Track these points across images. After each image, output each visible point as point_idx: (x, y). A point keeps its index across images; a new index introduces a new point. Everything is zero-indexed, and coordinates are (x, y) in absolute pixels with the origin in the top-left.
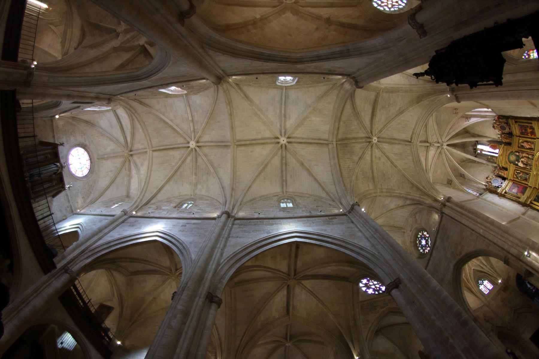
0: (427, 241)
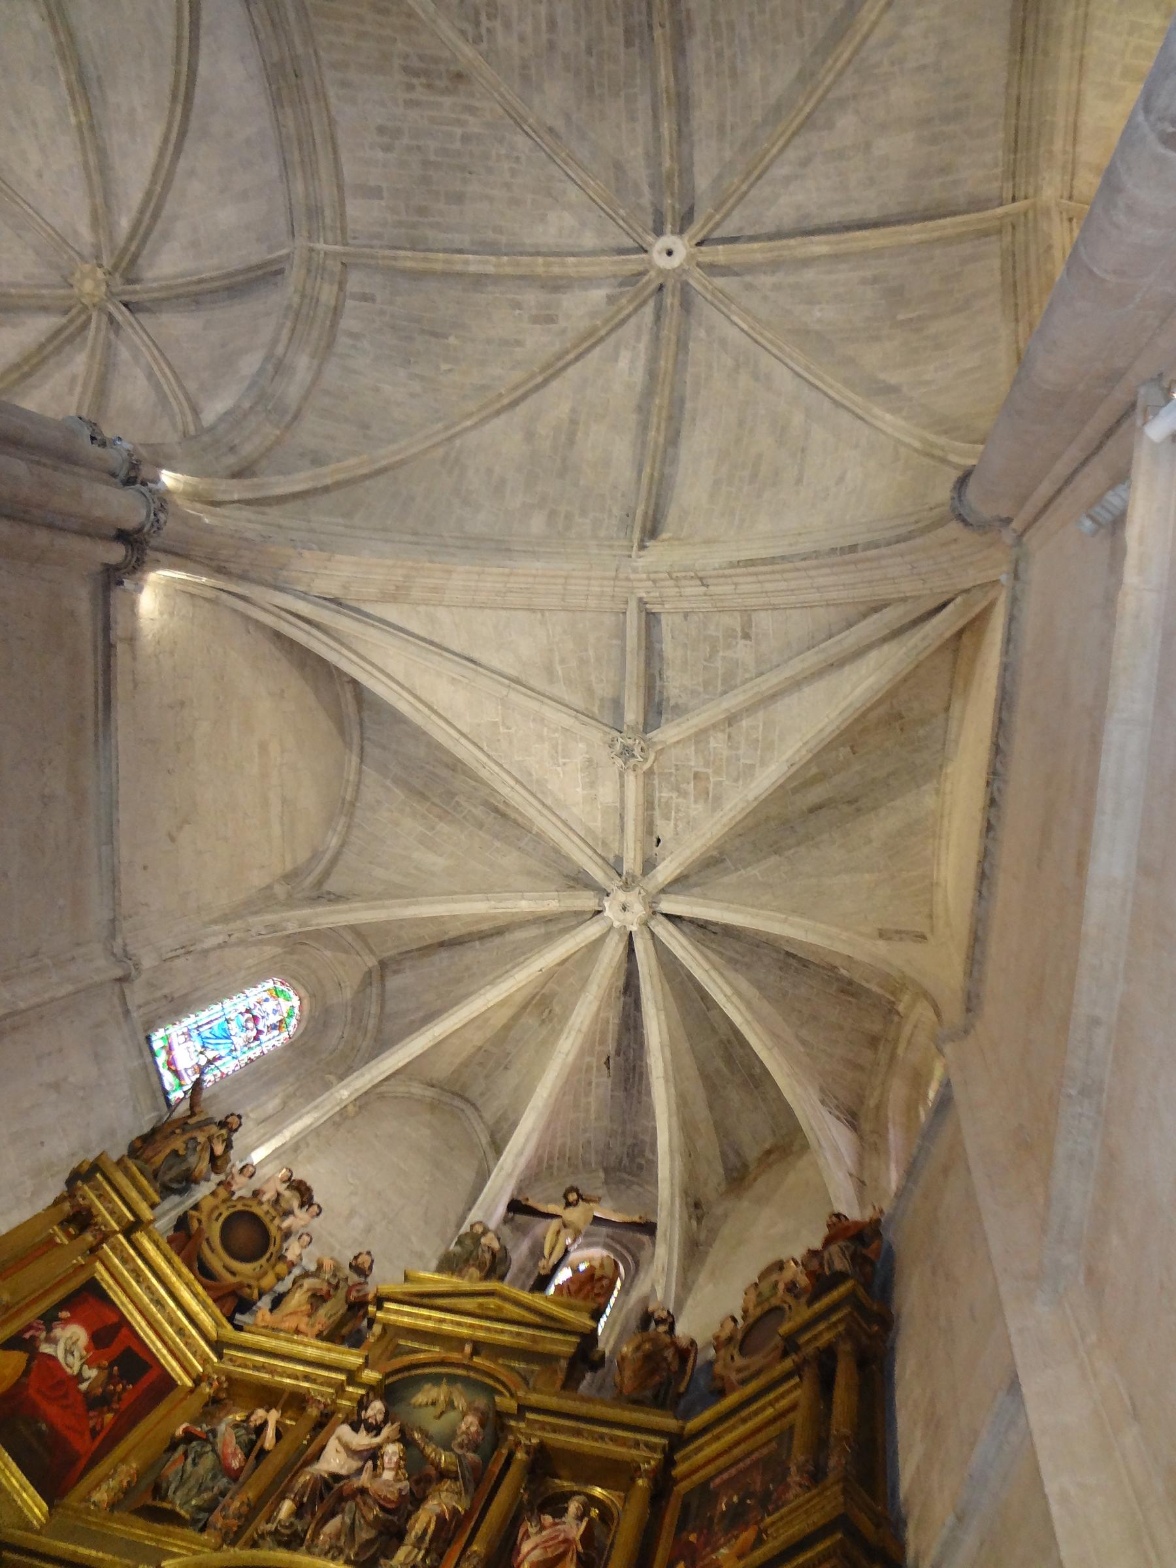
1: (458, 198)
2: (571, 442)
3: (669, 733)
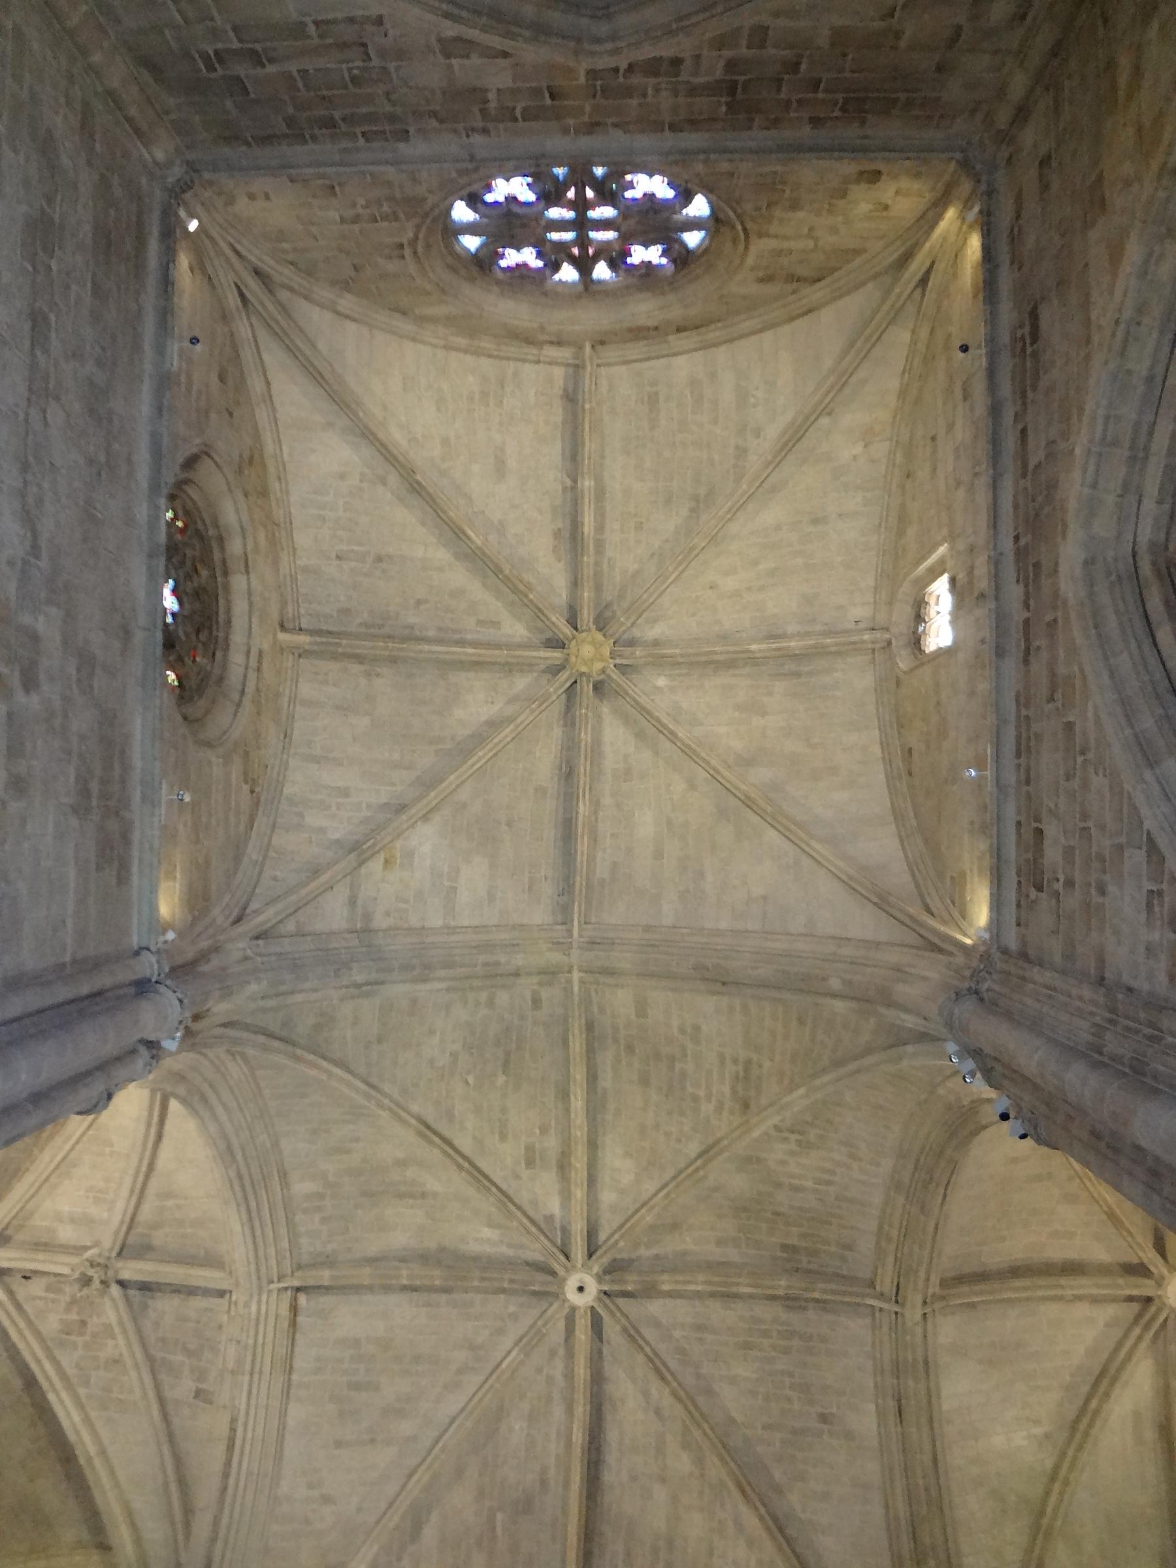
2: (401, 1196)
3: (111, 1310)
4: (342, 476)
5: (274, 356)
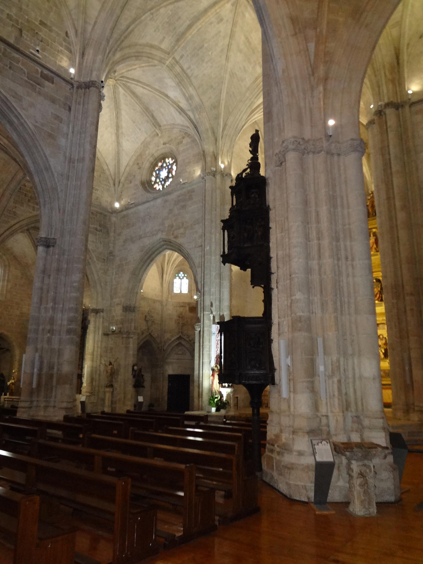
0: (167, 178)
1: (179, 18)
4: (128, 140)
5: (122, 169)
